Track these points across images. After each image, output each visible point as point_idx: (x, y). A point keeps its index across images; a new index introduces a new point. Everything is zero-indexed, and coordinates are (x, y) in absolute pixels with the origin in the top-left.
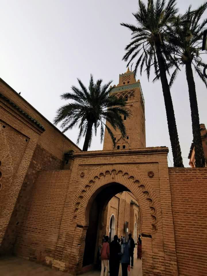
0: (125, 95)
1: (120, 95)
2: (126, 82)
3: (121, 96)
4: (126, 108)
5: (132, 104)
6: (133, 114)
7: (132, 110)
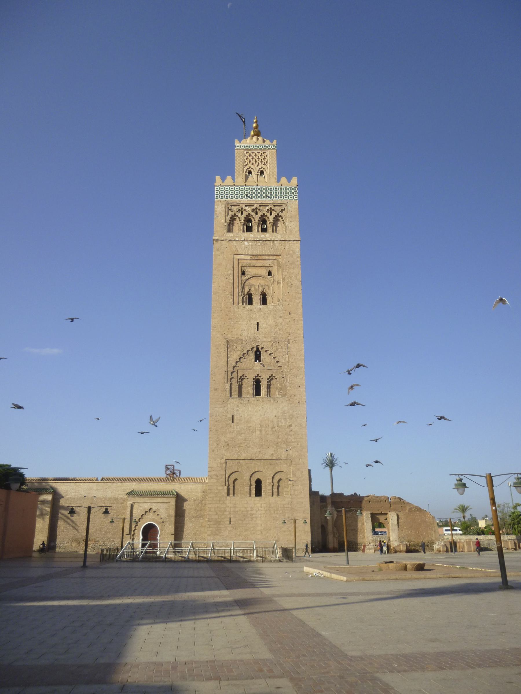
0: (260, 214)
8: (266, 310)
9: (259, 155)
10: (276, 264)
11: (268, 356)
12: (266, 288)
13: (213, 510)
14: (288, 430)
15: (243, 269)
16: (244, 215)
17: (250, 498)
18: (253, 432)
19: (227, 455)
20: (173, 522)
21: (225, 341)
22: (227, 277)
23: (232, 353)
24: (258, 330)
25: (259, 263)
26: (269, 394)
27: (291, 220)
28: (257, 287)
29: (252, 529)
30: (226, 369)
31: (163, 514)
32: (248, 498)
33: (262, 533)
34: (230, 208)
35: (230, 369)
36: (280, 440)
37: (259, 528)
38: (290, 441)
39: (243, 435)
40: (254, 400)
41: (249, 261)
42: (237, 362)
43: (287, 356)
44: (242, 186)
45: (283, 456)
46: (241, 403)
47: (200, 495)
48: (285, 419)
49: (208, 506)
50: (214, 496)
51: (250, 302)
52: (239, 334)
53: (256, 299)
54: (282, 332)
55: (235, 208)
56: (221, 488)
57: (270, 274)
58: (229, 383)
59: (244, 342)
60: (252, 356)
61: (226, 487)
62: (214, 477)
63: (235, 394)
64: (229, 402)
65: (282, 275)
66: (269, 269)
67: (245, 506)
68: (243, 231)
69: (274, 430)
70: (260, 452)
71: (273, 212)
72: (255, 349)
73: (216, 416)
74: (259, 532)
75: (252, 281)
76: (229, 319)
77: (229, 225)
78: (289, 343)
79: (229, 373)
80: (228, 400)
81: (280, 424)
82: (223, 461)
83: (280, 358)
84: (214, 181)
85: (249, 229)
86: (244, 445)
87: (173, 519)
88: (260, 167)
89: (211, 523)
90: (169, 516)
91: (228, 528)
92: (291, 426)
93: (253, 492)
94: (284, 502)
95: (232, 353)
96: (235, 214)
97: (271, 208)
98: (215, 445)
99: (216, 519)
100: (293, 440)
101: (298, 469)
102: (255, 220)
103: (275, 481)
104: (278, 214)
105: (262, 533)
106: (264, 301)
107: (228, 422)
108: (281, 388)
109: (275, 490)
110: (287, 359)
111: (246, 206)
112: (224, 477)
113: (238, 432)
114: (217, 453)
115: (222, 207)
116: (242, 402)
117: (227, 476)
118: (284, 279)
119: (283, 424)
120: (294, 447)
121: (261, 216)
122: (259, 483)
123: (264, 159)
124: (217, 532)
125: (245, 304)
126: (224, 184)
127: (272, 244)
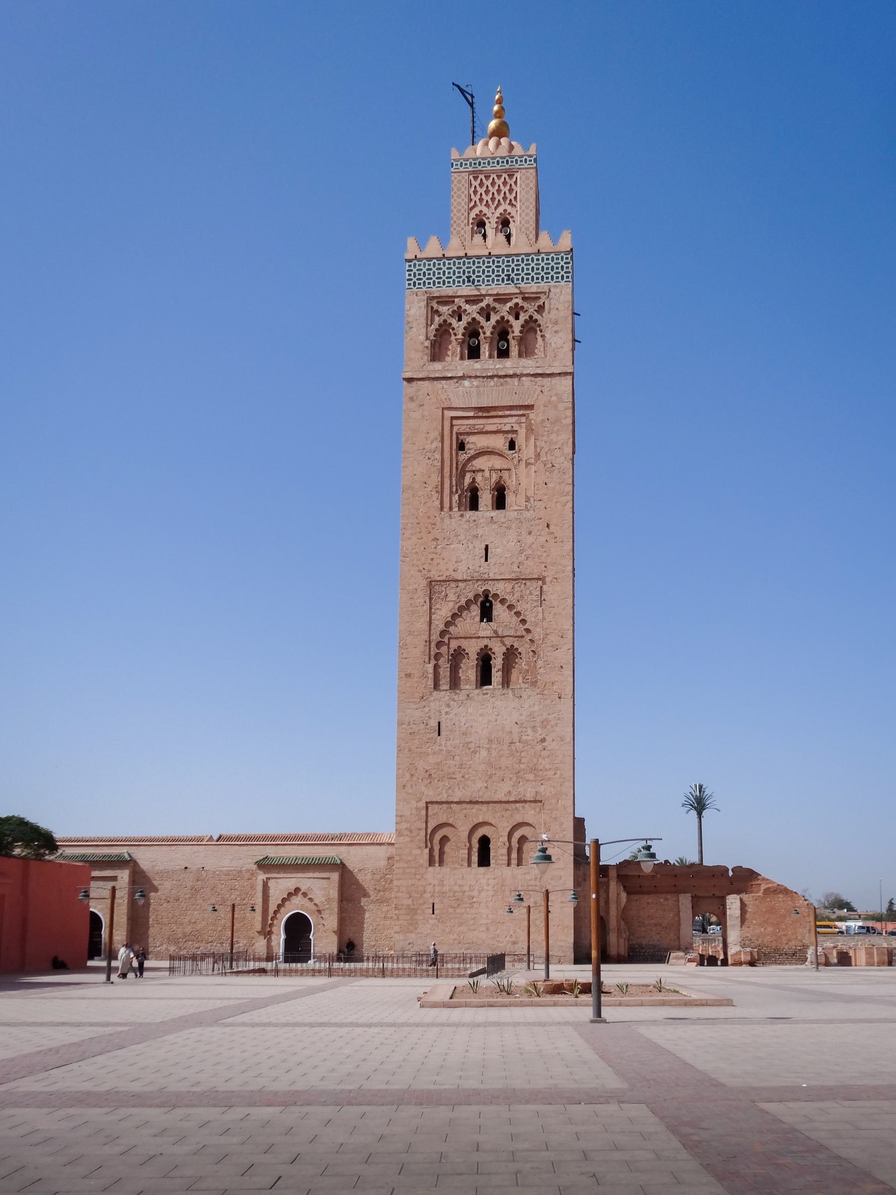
0: (494, 318)
8: (503, 520)
9: (499, 182)
10: (524, 425)
11: (504, 611)
12: (505, 475)
13: (404, 889)
14: (539, 747)
15: (461, 437)
16: (463, 323)
17: (469, 869)
18: (475, 752)
19: (431, 794)
20: (336, 910)
21: (424, 583)
22: (429, 455)
23: (438, 606)
24: (486, 560)
25: (492, 424)
26: (506, 682)
27: (556, 328)
28: (487, 474)
29: (472, 922)
30: (426, 637)
31: (319, 896)
32: (465, 870)
33: (488, 929)
34: (435, 306)
35: (435, 637)
36: (523, 766)
37: (483, 921)
38: (541, 767)
39: (457, 758)
40: (478, 695)
41: (471, 422)
42: (448, 624)
43: (540, 609)
44: (459, 258)
45: (529, 796)
46: (453, 700)
47: (383, 863)
48: (534, 727)
49: (395, 883)
50: (405, 865)
51: (474, 505)
52: (451, 569)
53: (486, 498)
54: (531, 564)
55: (444, 309)
56: (418, 852)
57: (512, 445)
58: (433, 662)
59: (460, 584)
60: (476, 610)
61: (427, 851)
62: (406, 833)
63: (445, 684)
64: (432, 699)
65: (536, 446)
66: (510, 436)
67: (460, 882)
68: (462, 358)
69: (513, 748)
70: (486, 788)
71: (522, 315)
72: (481, 599)
73: (409, 724)
74: (483, 928)
75: (478, 463)
76: (433, 540)
77: (433, 344)
78: (544, 583)
79: (433, 645)
80: (431, 694)
81: (524, 738)
82: (422, 804)
83: (527, 613)
84: (404, 248)
85: (474, 353)
86: (458, 776)
87: (335, 905)
89: (401, 912)
90: (329, 900)
91: (430, 921)
92: (543, 740)
93: (475, 858)
94: (528, 877)
95: (438, 606)
96: (445, 321)
97: (517, 304)
98: (408, 776)
99: (409, 906)
100: (548, 766)
101: (555, 818)
102: (484, 333)
103: (515, 844)
104: (531, 317)
105: (488, 929)
106: (500, 502)
107: (431, 735)
108: (527, 671)
109: (514, 855)
110: (540, 616)
111: (467, 302)
112: (423, 833)
113: (449, 751)
114: (410, 791)
115: (420, 308)
116: (456, 697)
117: (429, 832)
118: (538, 456)
119: (529, 738)
120: (549, 779)
121: (497, 322)
122: (485, 842)
124: (411, 928)
125: (463, 508)
126: (424, 255)
127: (516, 384)
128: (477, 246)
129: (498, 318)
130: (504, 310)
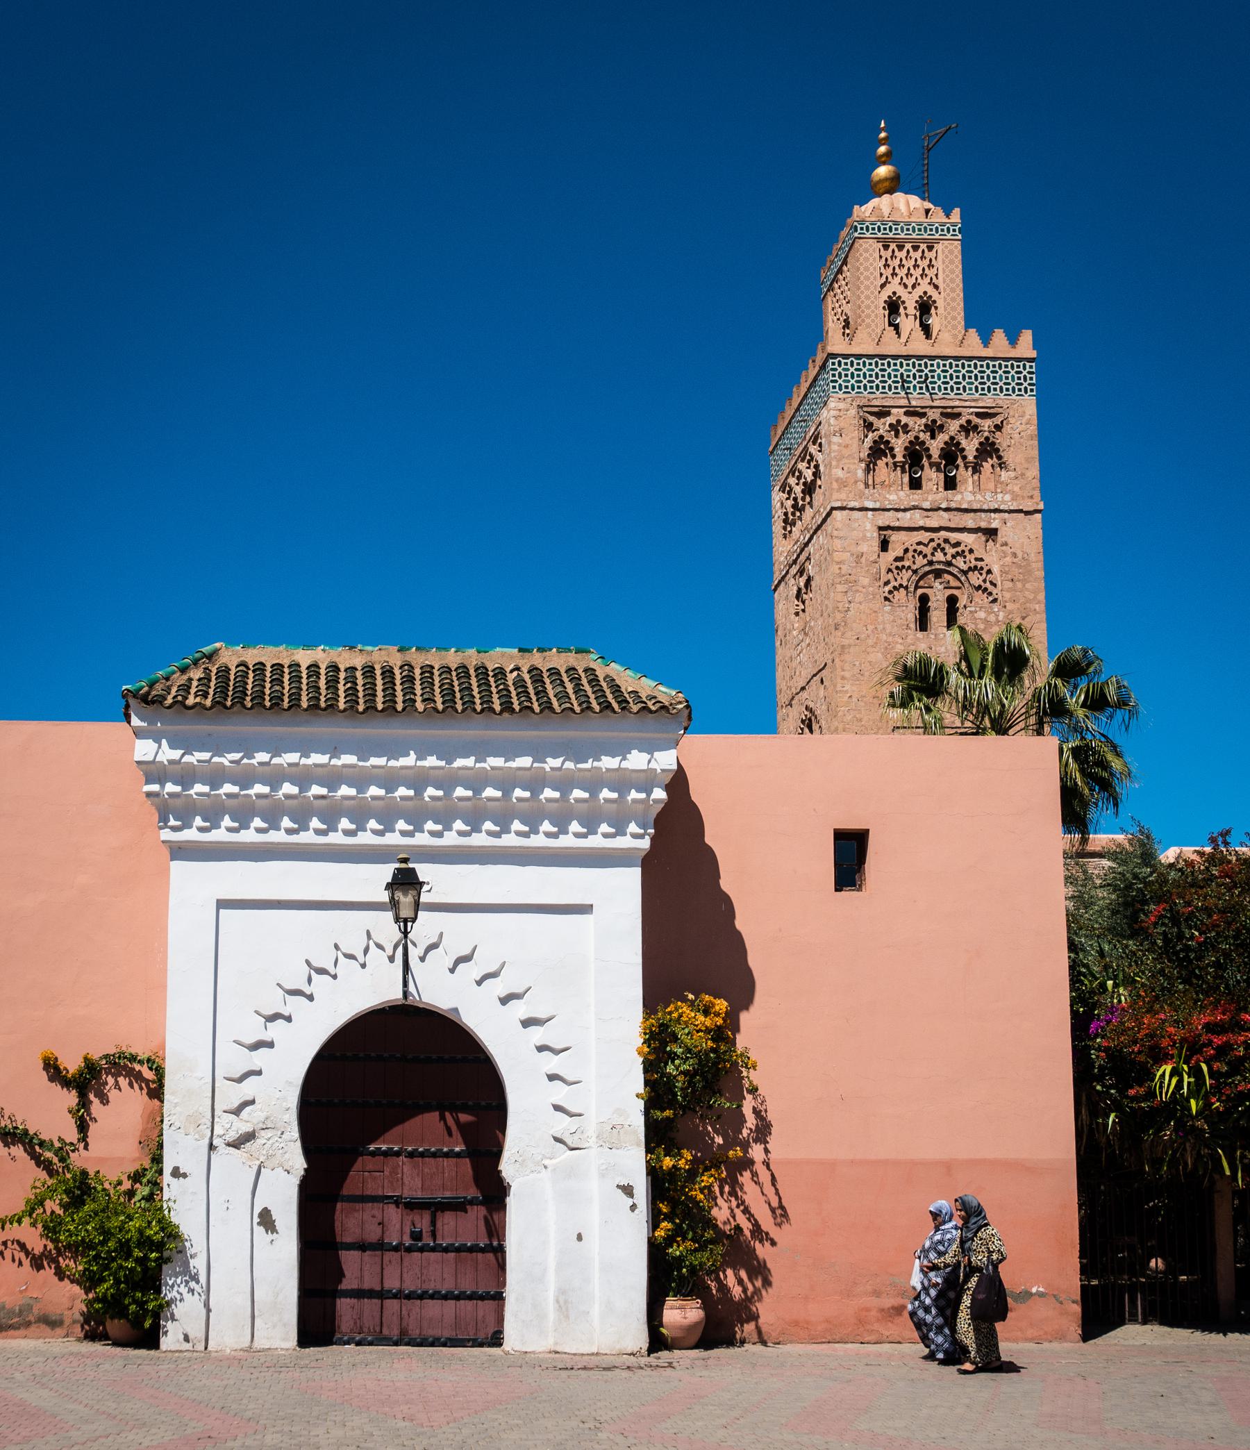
0: (942, 438)
1: (906, 425)
2: (910, 302)
3: (917, 438)
4: (958, 544)
5: (993, 526)
6: (1007, 595)
7: (995, 569)
88: (919, 292)
123: (930, 266)
128: (892, 345)
129: (947, 438)
130: (953, 426)
